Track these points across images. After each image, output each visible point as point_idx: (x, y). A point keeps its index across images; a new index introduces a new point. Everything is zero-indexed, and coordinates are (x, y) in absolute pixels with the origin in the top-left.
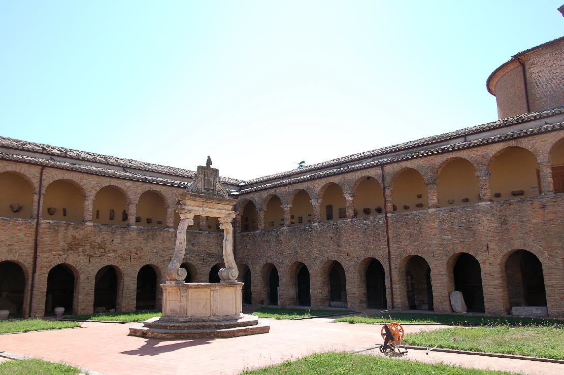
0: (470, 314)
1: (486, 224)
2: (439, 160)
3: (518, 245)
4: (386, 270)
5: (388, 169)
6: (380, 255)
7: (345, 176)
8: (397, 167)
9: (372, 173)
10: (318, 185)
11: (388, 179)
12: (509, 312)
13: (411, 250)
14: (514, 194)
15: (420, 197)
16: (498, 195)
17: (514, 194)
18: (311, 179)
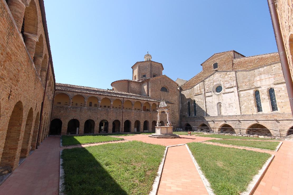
0: (113, 133)
1: (142, 115)
2: (136, 101)
3: (147, 119)
4: (121, 123)
5: (124, 99)
6: (120, 119)
7: (112, 97)
8: (127, 99)
9: (121, 99)
10: (102, 97)
11: (124, 101)
12: (144, 131)
13: (128, 119)
14: (138, 109)
15: (120, 106)
16: (135, 109)
17: (138, 109)
18: (100, 94)
